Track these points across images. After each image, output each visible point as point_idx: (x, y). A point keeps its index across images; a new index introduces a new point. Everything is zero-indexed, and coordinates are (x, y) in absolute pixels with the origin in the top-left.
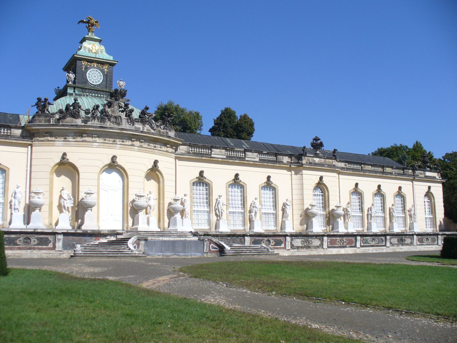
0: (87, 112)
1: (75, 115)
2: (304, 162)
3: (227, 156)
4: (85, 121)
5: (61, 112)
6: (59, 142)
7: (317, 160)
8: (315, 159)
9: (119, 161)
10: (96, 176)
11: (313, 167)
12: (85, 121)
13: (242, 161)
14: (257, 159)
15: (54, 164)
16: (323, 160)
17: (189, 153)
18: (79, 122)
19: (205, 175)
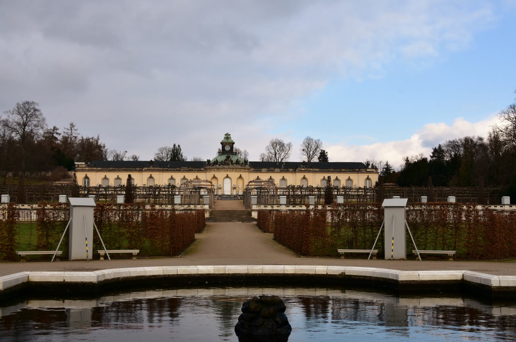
0: (220, 162)
1: (217, 164)
2: (297, 170)
3: (268, 171)
4: (219, 165)
5: (213, 163)
6: (213, 172)
7: (303, 169)
8: (302, 169)
9: (229, 176)
10: (222, 180)
11: (301, 171)
12: (219, 165)
13: (273, 171)
14: (279, 171)
15: (211, 177)
16: (306, 169)
17: (254, 171)
18: (218, 165)
19: (259, 177)
